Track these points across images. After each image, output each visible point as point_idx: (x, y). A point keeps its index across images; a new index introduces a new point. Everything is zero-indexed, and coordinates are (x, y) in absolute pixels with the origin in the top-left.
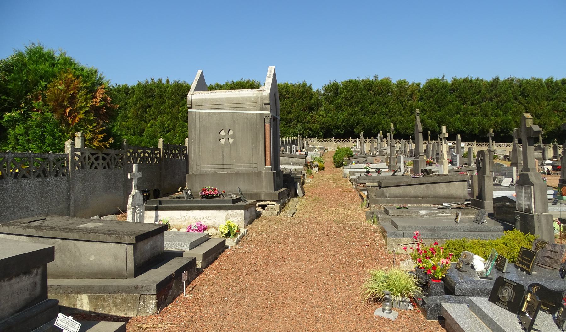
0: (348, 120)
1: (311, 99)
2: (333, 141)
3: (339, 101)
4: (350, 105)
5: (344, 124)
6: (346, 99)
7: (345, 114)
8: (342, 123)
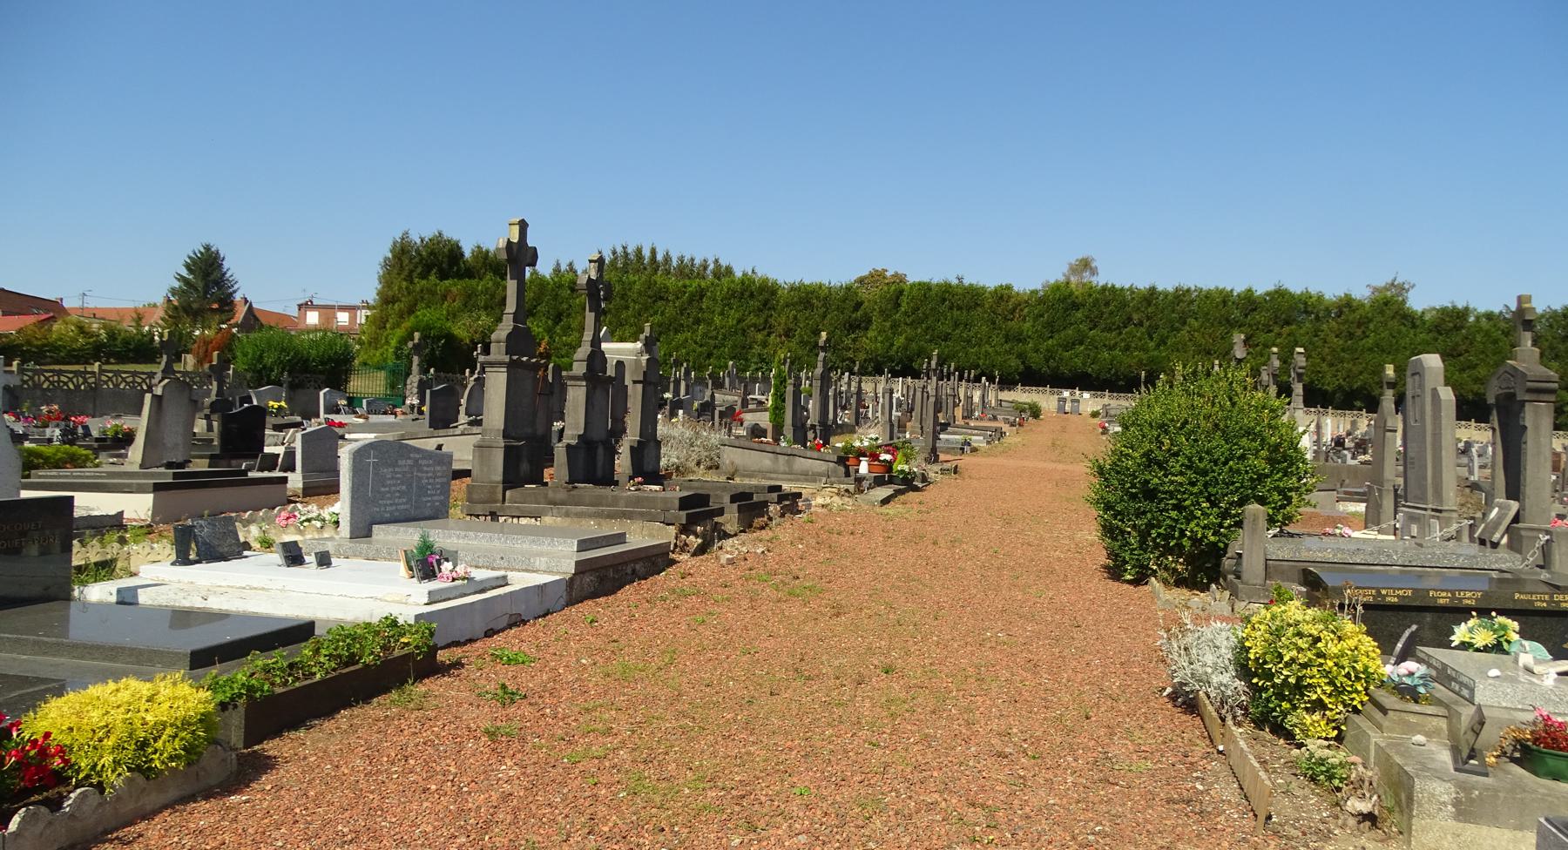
6: (906, 313)
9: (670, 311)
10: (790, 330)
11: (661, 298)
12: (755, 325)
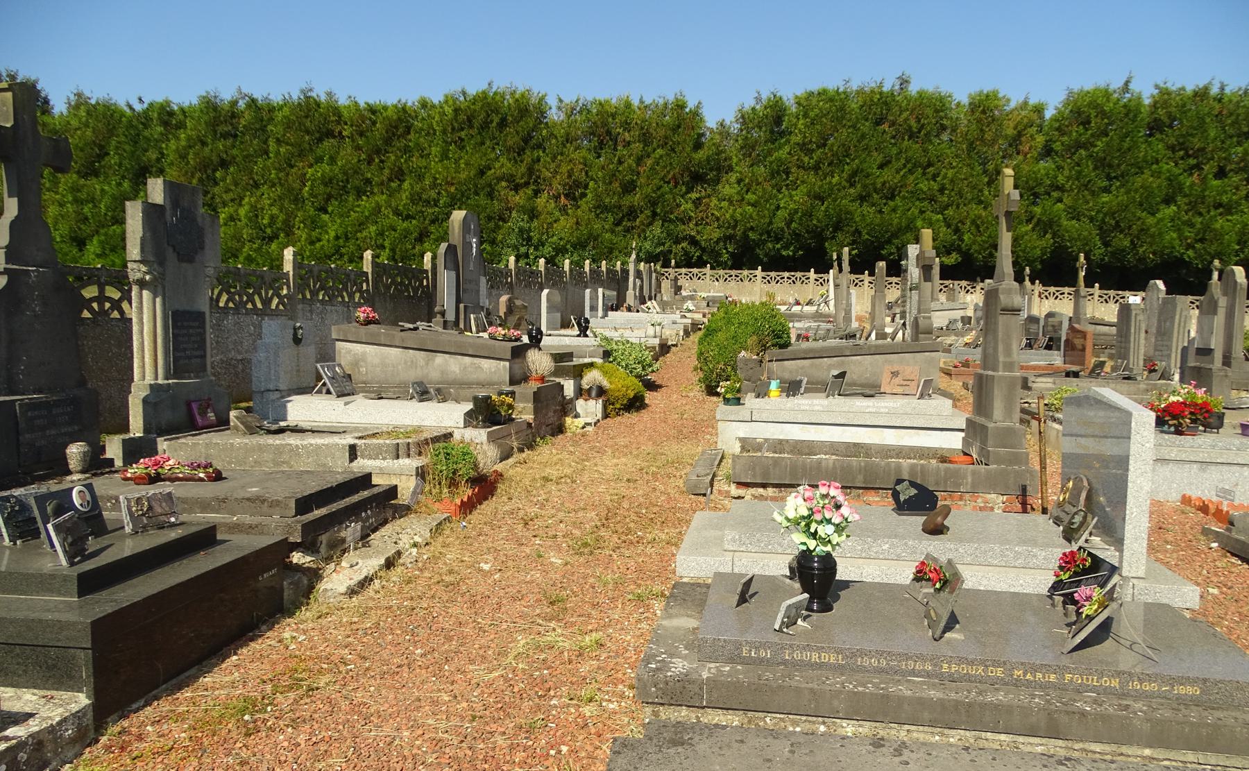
0: (809, 214)
1: (698, 146)
2: (759, 278)
3: (783, 153)
4: (816, 168)
5: (794, 225)
6: (804, 147)
7: (799, 195)
8: (788, 224)
9: (347, 155)
10: (577, 184)
11: (330, 134)
12: (510, 179)
